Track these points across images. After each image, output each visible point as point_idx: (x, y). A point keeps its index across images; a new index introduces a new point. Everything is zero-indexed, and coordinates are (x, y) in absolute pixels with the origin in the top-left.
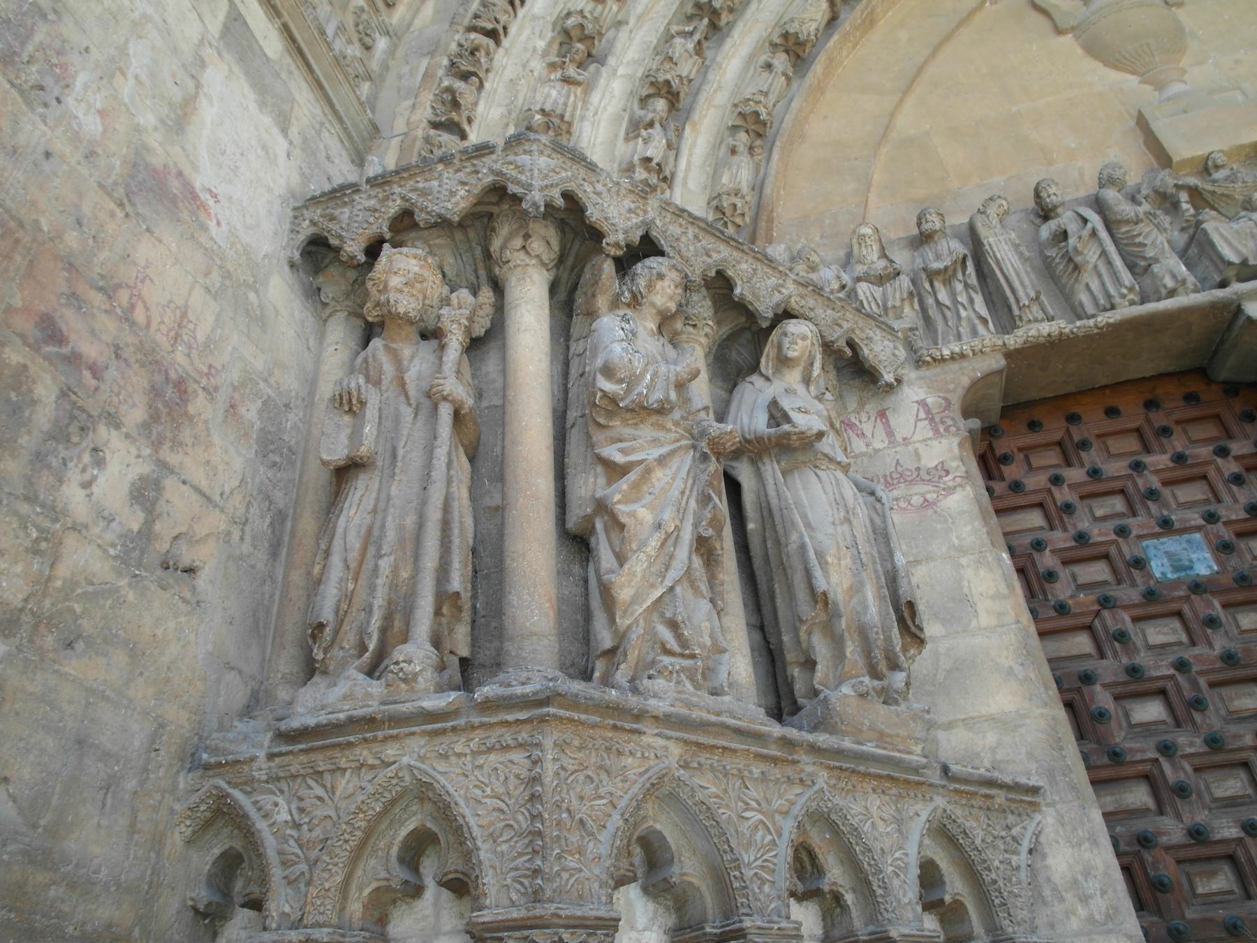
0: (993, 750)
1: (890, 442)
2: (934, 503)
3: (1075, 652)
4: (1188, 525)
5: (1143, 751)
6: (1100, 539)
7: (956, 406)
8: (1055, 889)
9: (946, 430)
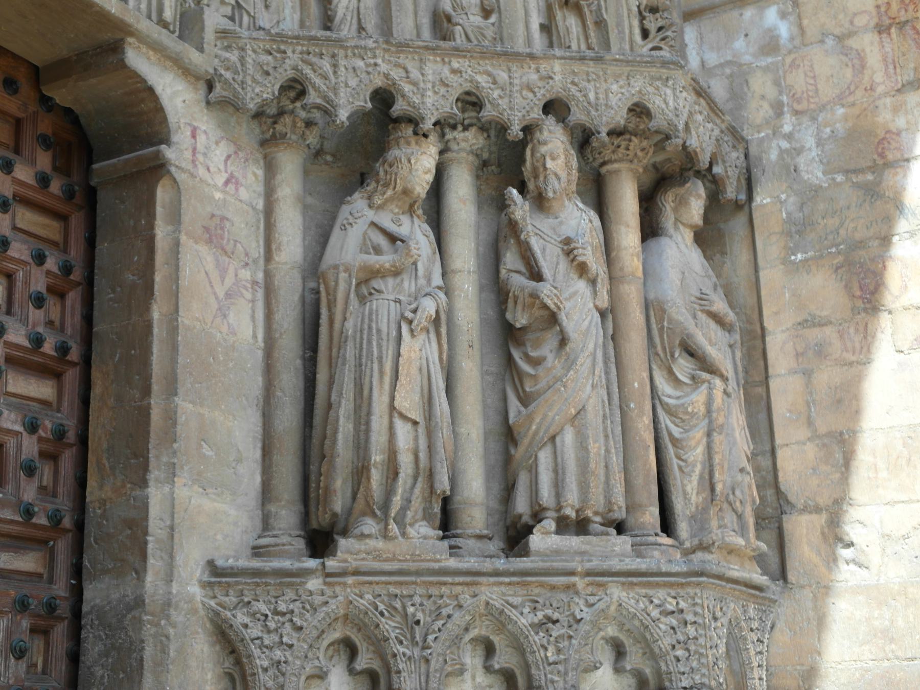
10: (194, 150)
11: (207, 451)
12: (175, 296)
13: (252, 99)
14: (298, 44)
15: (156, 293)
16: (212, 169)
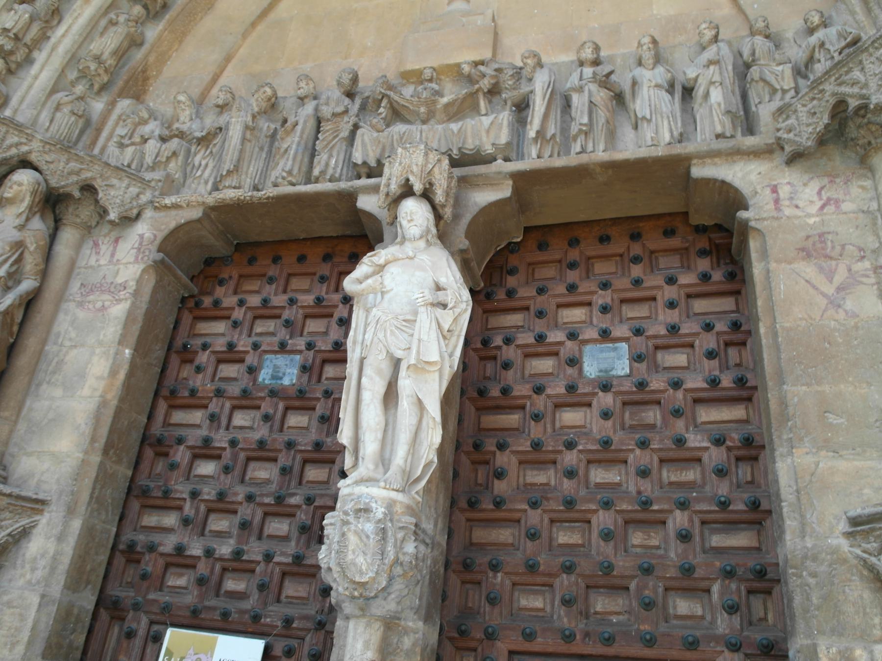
0: (42, 474)
1: (110, 261)
2: (106, 309)
3: (191, 422)
4: (295, 348)
5: (182, 492)
6: (241, 349)
7: (158, 242)
8: (23, 561)
9: (142, 259)
10: (777, 201)
11: (832, 418)
12: (771, 310)
13: (808, 139)
14: (830, 76)
15: (760, 314)
16: (801, 204)
